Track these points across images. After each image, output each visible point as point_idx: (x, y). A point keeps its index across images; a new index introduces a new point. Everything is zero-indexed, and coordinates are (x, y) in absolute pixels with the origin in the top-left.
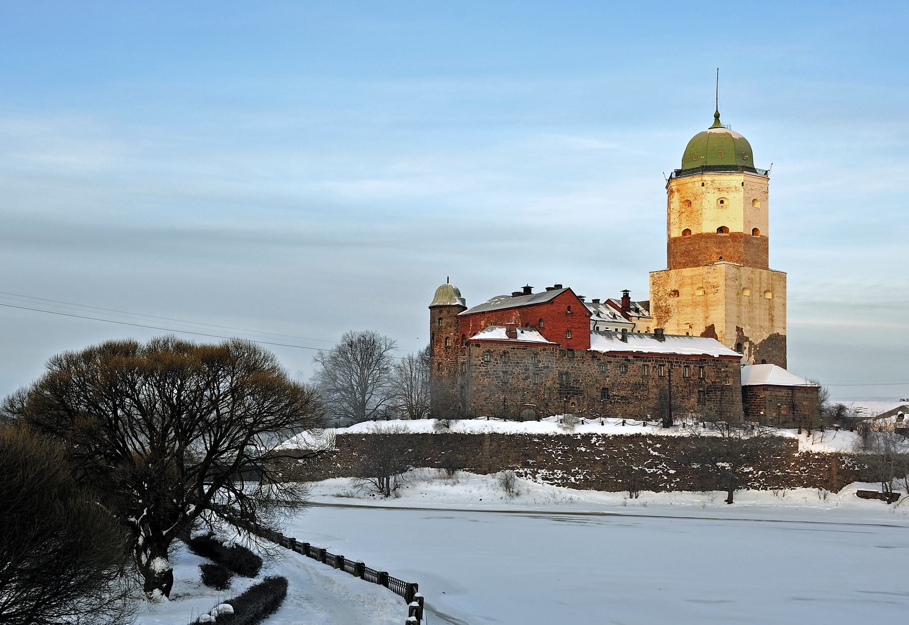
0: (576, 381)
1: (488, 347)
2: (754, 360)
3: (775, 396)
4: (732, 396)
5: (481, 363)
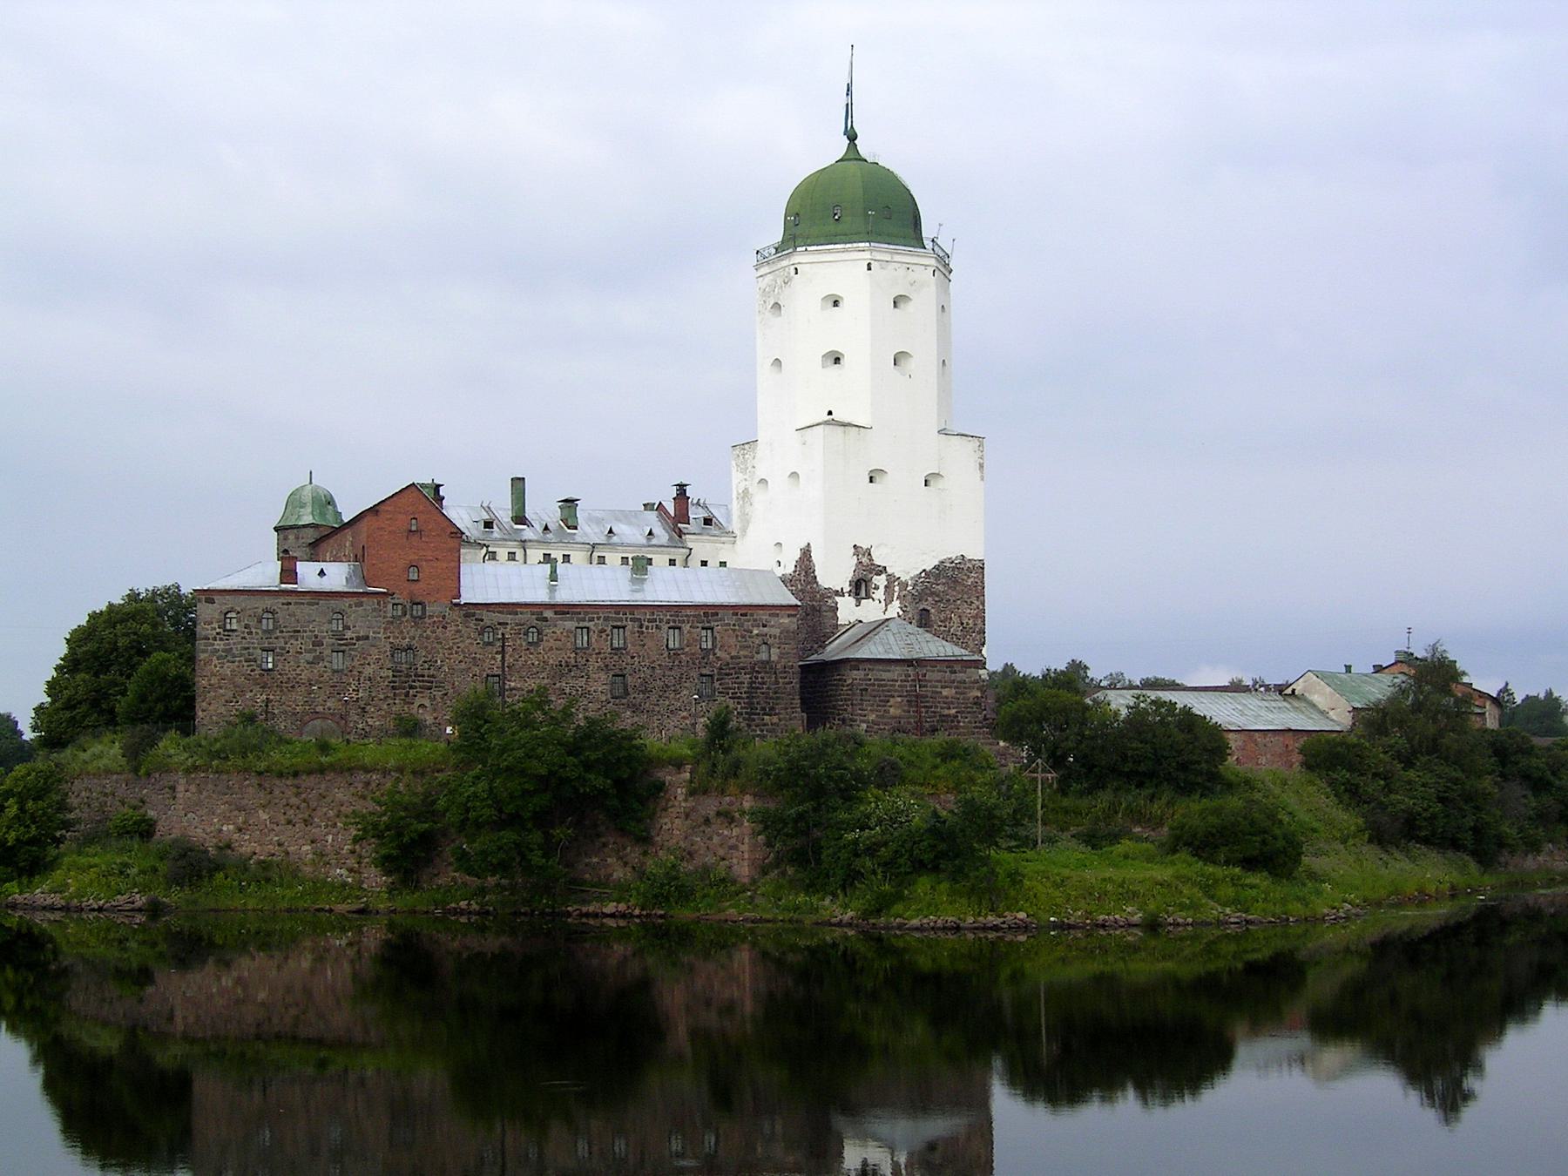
0: (432, 663)
1: (230, 601)
2: (899, 610)
3: (877, 680)
4: (777, 682)
5: (218, 634)
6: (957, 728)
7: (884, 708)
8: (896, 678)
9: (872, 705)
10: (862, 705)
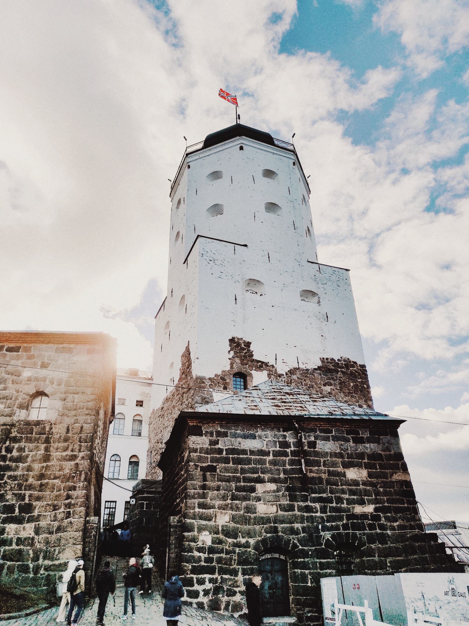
4: (47, 458)
7: (244, 503)
8: (264, 448)
10: (204, 496)
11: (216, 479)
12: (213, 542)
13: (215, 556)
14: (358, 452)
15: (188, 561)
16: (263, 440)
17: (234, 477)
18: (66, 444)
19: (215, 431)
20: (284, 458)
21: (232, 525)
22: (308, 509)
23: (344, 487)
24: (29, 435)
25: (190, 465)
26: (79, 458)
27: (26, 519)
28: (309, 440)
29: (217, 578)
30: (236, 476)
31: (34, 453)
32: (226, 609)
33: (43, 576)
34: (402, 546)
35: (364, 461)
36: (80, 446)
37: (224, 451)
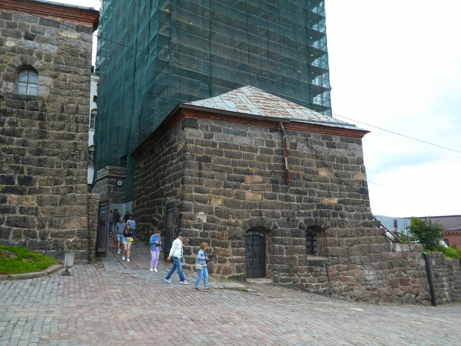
3: (226, 145)
4: (43, 134)
6: (342, 224)
7: (235, 191)
9: (217, 185)
10: (200, 183)
11: (211, 169)
12: (208, 220)
13: (210, 232)
14: (329, 155)
15: (186, 234)
16: (252, 138)
17: (226, 168)
18: (62, 123)
19: (210, 126)
20: (270, 155)
21: (224, 207)
22: (287, 199)
23: (317, 183)
24: (20, 110)
25: (187, 155)
26: (77, 138)
27: (28, 191)
28: (292, 142)
29: (211, 249)
30: (229, 167)
31: (28, 128)
32: (218, 272)
33: (51, 241)
34: (355, 229)
35: (333, 162)
36: (77, 126)
37: (218, 144)
